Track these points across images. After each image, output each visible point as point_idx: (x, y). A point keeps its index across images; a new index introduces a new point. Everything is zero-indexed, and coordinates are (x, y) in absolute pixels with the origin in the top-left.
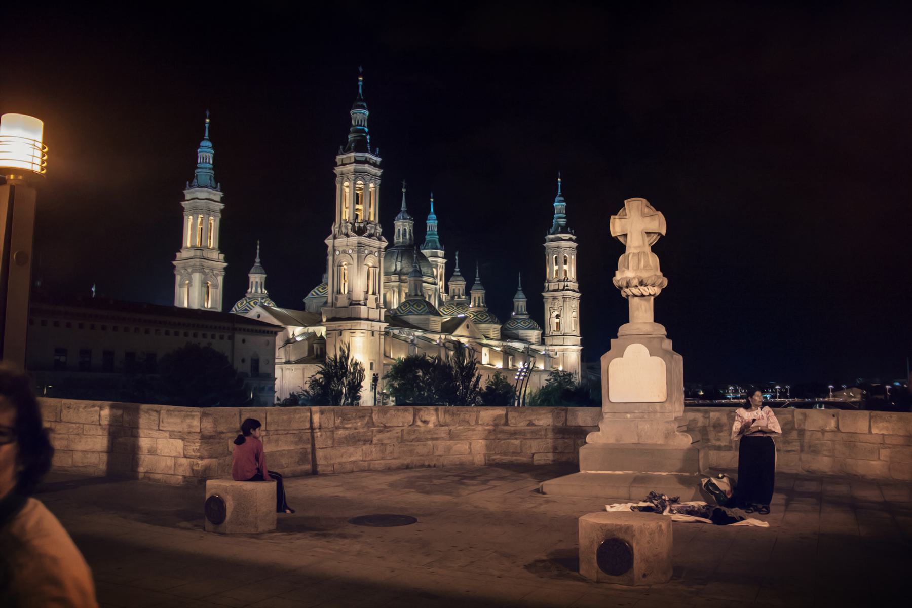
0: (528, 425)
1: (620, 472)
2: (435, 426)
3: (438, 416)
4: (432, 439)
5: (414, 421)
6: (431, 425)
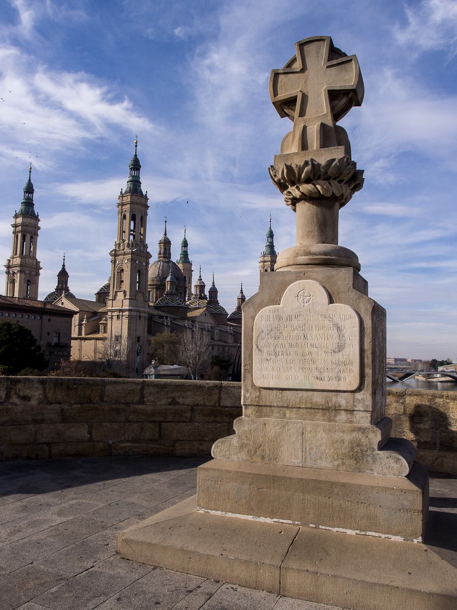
0: (169, 404)
1: (269, 520)
2: (40, 403)
3: (44, 389)
4: (36, 422)
5: (8, 396)
6: (34, 402)
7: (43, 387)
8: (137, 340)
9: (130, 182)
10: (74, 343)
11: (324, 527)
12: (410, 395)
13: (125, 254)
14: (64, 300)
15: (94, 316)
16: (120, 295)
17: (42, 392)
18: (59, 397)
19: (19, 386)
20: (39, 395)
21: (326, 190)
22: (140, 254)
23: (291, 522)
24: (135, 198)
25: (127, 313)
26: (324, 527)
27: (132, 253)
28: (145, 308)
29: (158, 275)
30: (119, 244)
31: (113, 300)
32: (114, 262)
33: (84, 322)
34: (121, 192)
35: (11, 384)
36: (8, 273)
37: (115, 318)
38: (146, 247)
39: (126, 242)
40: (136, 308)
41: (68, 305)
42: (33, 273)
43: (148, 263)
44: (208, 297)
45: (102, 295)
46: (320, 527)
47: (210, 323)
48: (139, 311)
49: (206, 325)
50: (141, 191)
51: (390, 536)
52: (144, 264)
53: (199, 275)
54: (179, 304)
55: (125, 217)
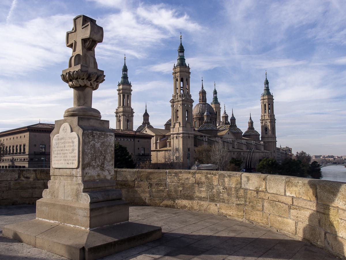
2: (34, 180)
3: (36, 174)
4: (33, 188)
5: (19, 177)
6: (31, 180)
7: (35, 173)
8: (188, 150)
9: (179, 59)
10: (153, 153)
11: (66, 224)
12: (197, 173)
13: (178, 101)
14: (147, 130)
15: (164, 138)
16: (177, 125)
17: (35, 175)
18: (43, 177)
19: (24, 172)
20: (33, 176)
21: (76, 84)
22: (187, 100)
23: (58, 222)
24: (182, 69)
25: (181, 135)
26: (66, 224)
27: (183, 100)
28: (192, 132)
29: (200, 112)
30: (175, 96)
31: (173, 128)
32: (173, 106)
33: (158, 141)
34: (174, 66)
35: (20, 171)
36: (117, 116)
37: (175, 138)
38: (190, 96)
39: (179, 94)
40: (186, 132)
41: (149, 132)
42: (130, 116)
43: (192, 106)
44: (230, 123)
45: (168, 125)
46: (65, 224)
47: (231, 139)
48: (188, 134)
49: (229, 139)
50: (185, 64)
51: (82, 227)
52: (190, 106)
53: (224, 110)
54: (212, 128)
55: (177, 80)
